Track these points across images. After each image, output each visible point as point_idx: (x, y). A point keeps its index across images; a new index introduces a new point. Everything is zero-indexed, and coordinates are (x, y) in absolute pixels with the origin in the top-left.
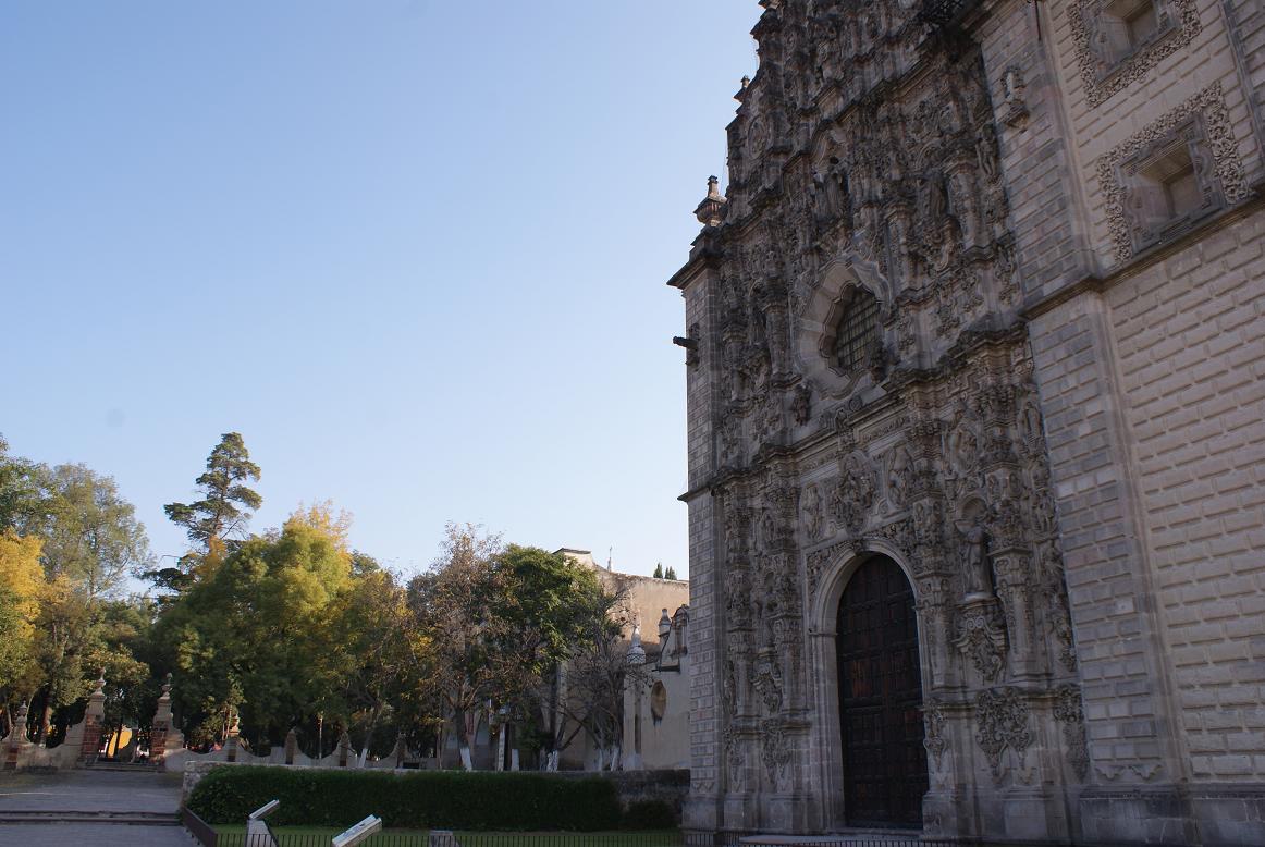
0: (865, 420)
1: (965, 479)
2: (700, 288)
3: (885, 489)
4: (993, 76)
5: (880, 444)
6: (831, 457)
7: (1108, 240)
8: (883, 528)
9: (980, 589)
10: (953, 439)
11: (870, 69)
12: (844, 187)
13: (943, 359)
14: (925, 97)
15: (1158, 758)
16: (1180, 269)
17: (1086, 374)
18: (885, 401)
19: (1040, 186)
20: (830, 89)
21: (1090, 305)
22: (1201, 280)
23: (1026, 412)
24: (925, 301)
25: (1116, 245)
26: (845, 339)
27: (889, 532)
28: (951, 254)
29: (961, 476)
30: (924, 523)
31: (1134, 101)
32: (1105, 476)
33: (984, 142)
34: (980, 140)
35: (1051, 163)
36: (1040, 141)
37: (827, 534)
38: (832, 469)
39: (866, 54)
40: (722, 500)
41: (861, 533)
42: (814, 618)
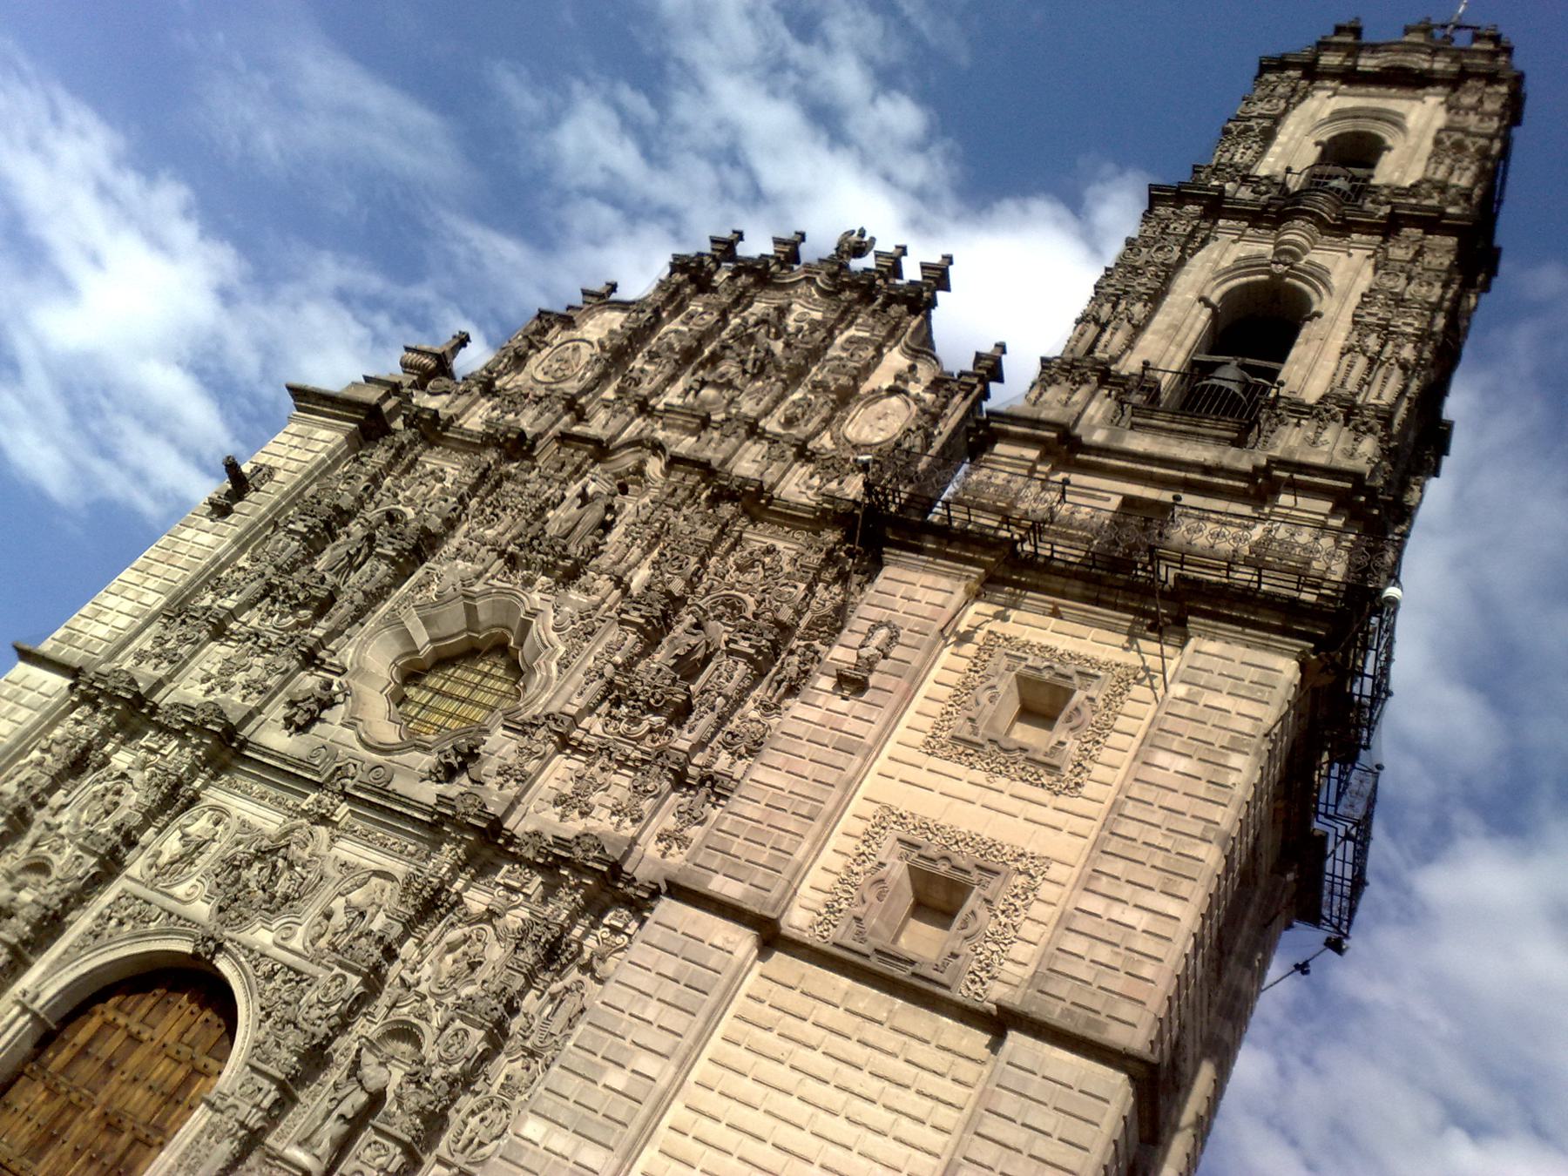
0: (371, 805)
1: (424, 998)
2: (323, 434)
5: (360, 850)
7: (821, 897)
8: (262, 955)
9: (318, 1152)
10: (454, 935)
11: (756, 450)
12: (606, 527)
13: (537, 834)
14: (780, 545)
16: (860, 1006)
18: (424, 812)
19: (808, 769)
20: (694, 416)
21: (742, 941)
22: (871, 1039)
24: (576, 750)
25: (823, 910)
26: (433, 681)
27: (265, 968)
28: (651, 731)
29: (423, 988)
30: (328, 1005)
31: (962, 788)
33: (795, 659)
34: (792, 652)
35: (841, 759)
36: (850, 725)
37: (180, 891)
38: (269, 821)
39: (764, 430)
40: (74, 706)
41: (227, 933)
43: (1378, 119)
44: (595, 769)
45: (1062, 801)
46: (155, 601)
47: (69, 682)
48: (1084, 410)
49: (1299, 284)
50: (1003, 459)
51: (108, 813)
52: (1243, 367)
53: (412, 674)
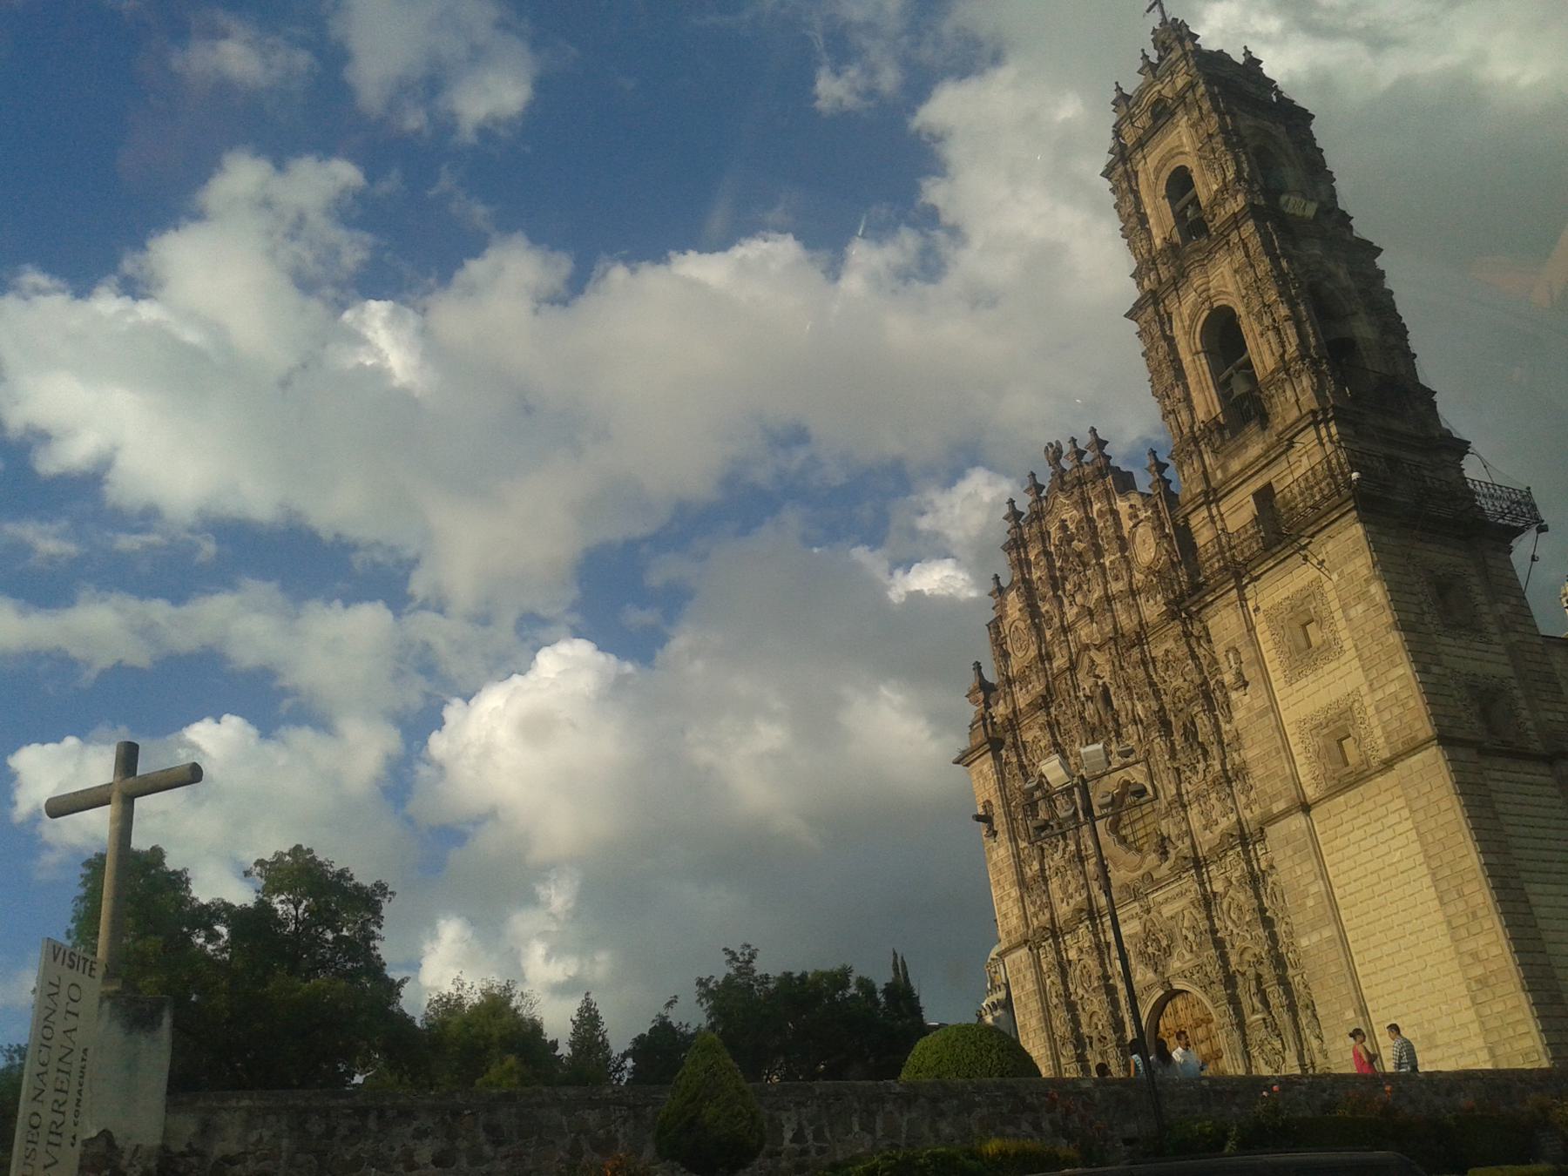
0: (1157, 890)
3: (1180, 942)
4: (1219, 649)
6: (1132, 917)
23: (1272, 888)
27: (1188, 975)
31: (1313, 687)
33: (1218, 693)
45: (1343, 660)
46: (1015, 892)
47: (1026, 949)
48: (1205, 467)
51: (1090, 976)
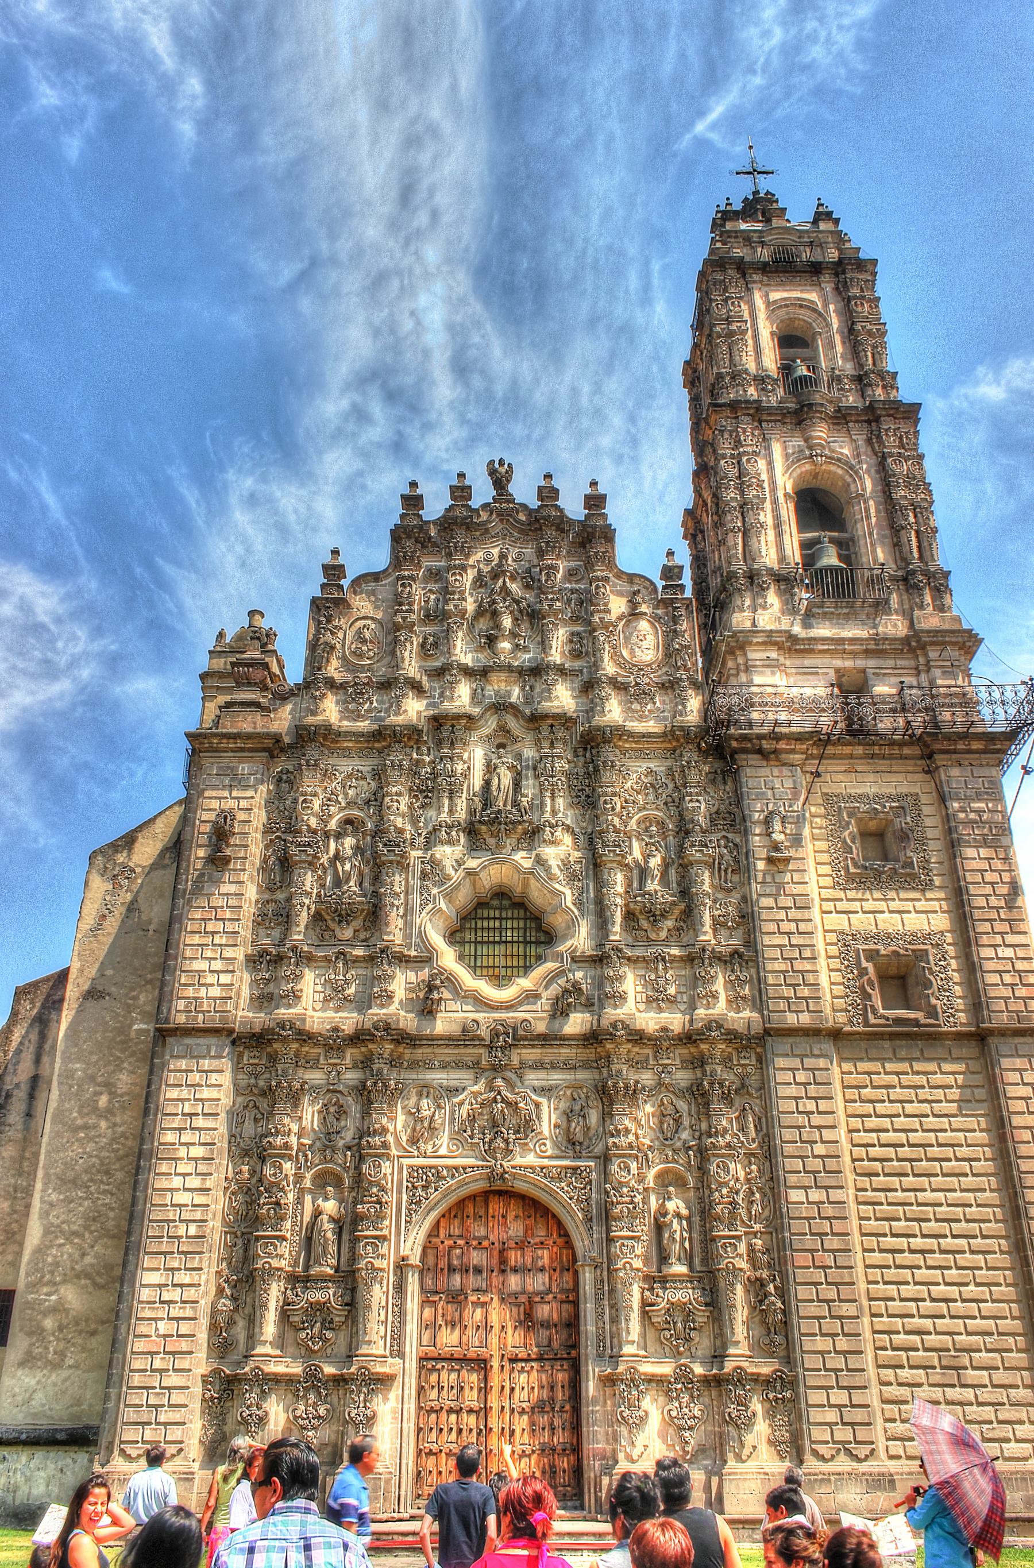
0: (533, 1046)
5: (542, 1075)
14: (652, 765)
15: (872, 1443)
17: (823, 1105)
32: (836, 1195)
35: (806, 914)
40: (240, 1055)
42: (409, 1244)
43: (801, 306)
44: (661, 973)
49: (833, 468)
50: (758, 663)
52: (832, 541)
53: (453, 936)
